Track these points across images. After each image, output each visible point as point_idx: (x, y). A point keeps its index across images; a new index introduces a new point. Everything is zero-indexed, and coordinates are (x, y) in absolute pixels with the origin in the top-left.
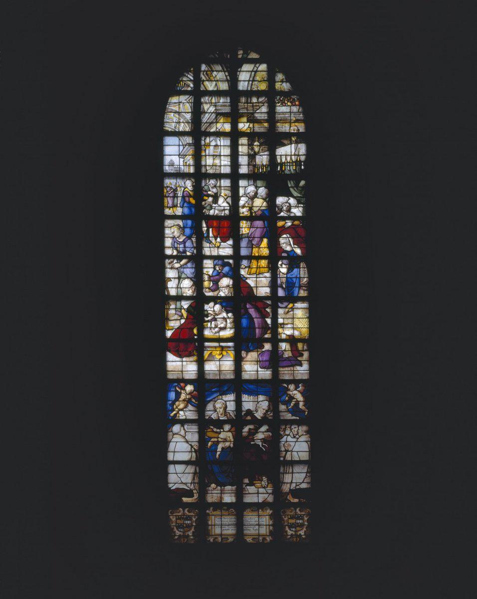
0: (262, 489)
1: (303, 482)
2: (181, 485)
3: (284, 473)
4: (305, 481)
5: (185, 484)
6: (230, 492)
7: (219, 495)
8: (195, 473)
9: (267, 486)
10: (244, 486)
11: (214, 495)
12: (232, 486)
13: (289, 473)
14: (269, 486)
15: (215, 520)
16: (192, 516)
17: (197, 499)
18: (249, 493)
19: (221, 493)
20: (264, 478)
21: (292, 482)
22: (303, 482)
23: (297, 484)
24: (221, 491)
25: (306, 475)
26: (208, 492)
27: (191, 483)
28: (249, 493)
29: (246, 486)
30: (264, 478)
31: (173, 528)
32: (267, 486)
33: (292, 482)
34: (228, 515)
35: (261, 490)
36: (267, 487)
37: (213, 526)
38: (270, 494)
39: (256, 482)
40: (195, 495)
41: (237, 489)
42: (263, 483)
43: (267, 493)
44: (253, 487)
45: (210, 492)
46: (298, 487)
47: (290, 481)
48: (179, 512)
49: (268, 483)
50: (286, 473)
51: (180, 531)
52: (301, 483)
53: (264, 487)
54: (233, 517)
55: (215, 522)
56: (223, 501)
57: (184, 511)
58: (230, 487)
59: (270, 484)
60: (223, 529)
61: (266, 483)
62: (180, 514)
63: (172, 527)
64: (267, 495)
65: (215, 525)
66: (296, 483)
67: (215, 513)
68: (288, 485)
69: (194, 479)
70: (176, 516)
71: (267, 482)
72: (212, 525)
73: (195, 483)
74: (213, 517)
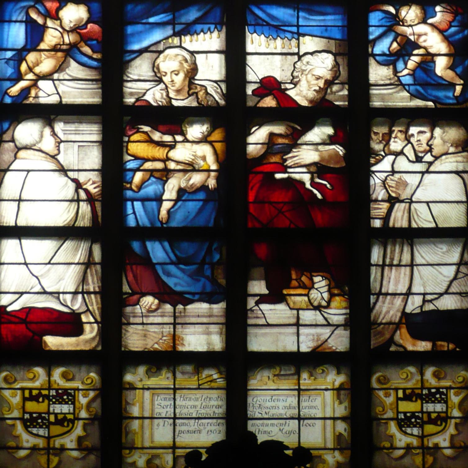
0: (312, 312)
1: (446, 292)
2: (43, 297)
3: (383, 266)
4: (452, 290)
5: (56, 295)
6: (205, 320)
7: (168, 329)
8: (88, 264)
9: (329, 302)
10: (251, 302)
11: (152, 328)
12: (210, 302)
13: (399, 265)
14: (333, 304)
15: (152, 401)
16: (78, 390)
17: (93, 339)
18: (268, 325)
19: (175, 324)
20: (317, 279)
21: (409, 293)
22: (446, 292)
23: (429, 297)
24: (175, 317)
25: (458, 272)
26: (132, 320)
27: (75, 293)
28: (268, 325)
29: (257, 303)
30: (317, 279)
31: (13, 425)
32: (329, 302)
33: (409, 293)
34: (198, 388)
35: (308, 316)
36: (328, 307)
37: (147, 422)
38: (338, 326)
39: (292, 292)
40: (87, 327)
41: (229, 313)
42: (314, 294)
43: (329, 325)
44: (281, 307)
45: (139, 320)
46: (429, 307)
47: (402, 288)
48: (33, 379)
49: (332, 295)
50: (391, 265)
51: (37, 435)
52: (441, 295)
53: (318, 308)
54: (214, 394)
55: (153, 410)
56: (180, 348)
57: (49, 375)
58: (205, 306)
59: (337, 298)
60: (178, 428)
61: (326, 296)
62: (37, 384)
63: (9, 422)
64: (326, 332)
65: (152, 418)
66: (424, 294)
67: (153, 382)
68: (398, 301)
69: (84, 280)
70: (23, 389)
71: (329, 291)
72: (143, 418)
73: (89, 293)
74: (147, 394)
